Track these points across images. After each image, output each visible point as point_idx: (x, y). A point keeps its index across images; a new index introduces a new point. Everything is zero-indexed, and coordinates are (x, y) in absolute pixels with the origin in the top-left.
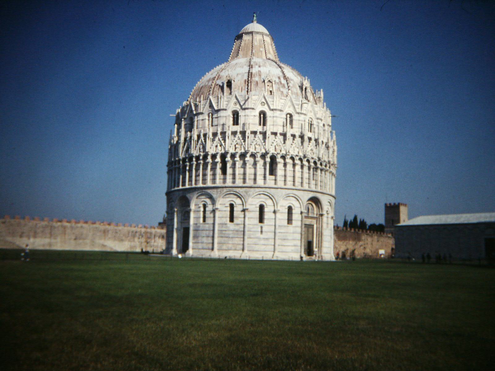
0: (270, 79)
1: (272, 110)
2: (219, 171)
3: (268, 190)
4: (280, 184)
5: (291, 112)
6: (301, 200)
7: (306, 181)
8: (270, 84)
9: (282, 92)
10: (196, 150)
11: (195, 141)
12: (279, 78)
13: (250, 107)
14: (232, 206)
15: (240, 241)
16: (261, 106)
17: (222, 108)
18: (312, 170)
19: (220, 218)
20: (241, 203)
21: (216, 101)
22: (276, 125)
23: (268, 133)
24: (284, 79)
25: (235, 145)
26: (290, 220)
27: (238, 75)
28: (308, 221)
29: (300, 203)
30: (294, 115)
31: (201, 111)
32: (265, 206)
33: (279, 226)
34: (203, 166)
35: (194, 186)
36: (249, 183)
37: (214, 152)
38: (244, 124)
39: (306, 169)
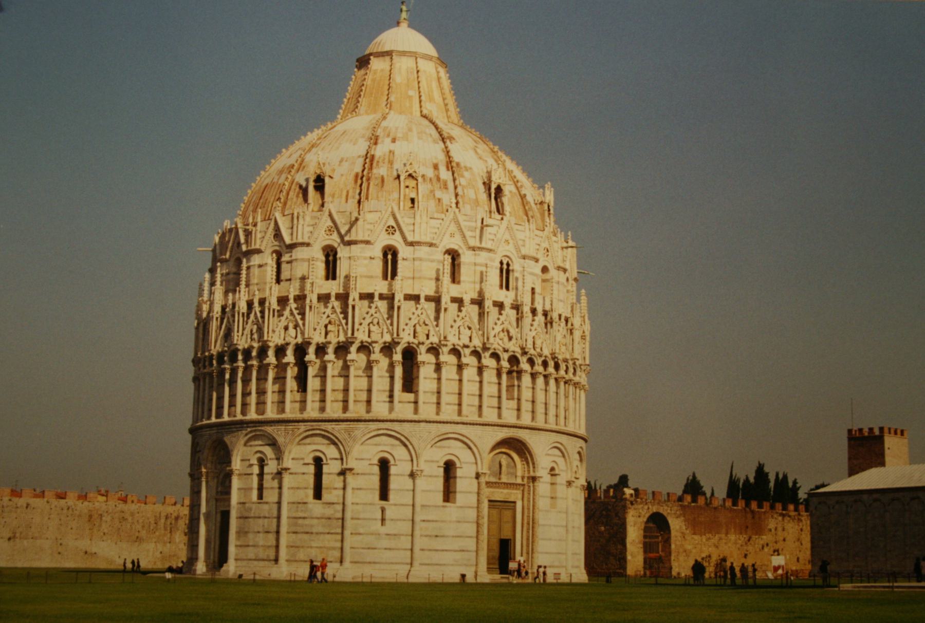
0: (411, 172)
1: (412, 244)
2: (291, 384)
3: (396, 426)
4: (427, 411)
5: (456, 247)
6: (475, 446)
7: (489, 402)
8: (412, 183)
9: (439, 200)
10: (244, 337)
11: (243, 314)
12: (436, 167)
13: (360, 238)
14: (318, 463)
15: (336, 541)
16: (387, 236)
17: (300, 240)
18: (504, 377)
19: (292, 491)
20: (338, 456)
21: (288, 224)
22: (420, 278)
23: (399, 297)
24: (448, 169)
25: (326, 326)
26: (448, 494)
27: (341, 161)
28: (500, 494)
29: (473, 452)
30: (464, 253)
31: (258, 247)
32: (392, 462)
33: (423, 506)
34: (258, 372)
35: (239, 417)
36: (356, 410)
37: (280, 342)
38: (347, 277)
39: (490, 376)
